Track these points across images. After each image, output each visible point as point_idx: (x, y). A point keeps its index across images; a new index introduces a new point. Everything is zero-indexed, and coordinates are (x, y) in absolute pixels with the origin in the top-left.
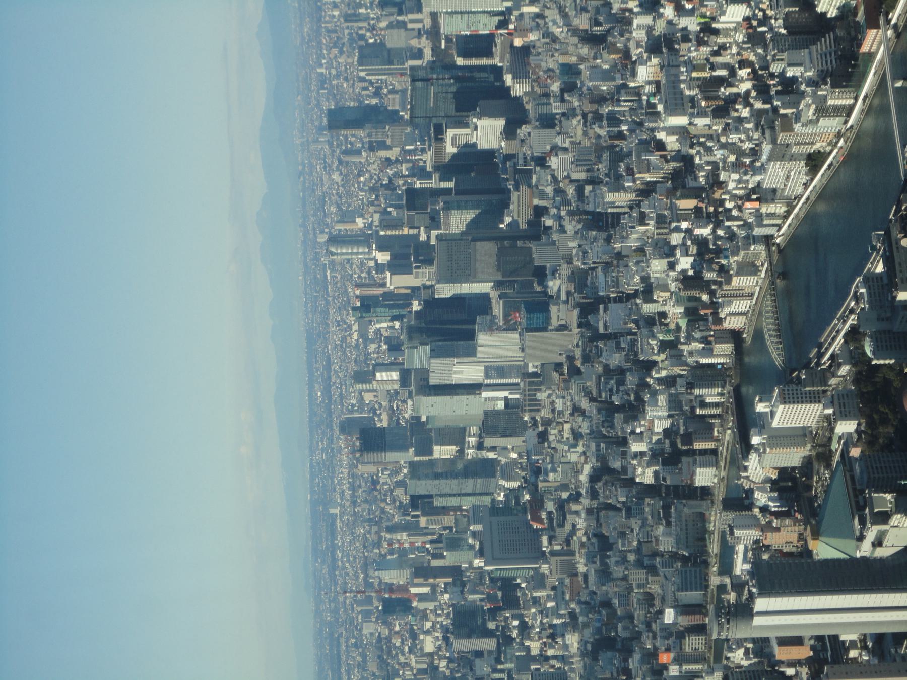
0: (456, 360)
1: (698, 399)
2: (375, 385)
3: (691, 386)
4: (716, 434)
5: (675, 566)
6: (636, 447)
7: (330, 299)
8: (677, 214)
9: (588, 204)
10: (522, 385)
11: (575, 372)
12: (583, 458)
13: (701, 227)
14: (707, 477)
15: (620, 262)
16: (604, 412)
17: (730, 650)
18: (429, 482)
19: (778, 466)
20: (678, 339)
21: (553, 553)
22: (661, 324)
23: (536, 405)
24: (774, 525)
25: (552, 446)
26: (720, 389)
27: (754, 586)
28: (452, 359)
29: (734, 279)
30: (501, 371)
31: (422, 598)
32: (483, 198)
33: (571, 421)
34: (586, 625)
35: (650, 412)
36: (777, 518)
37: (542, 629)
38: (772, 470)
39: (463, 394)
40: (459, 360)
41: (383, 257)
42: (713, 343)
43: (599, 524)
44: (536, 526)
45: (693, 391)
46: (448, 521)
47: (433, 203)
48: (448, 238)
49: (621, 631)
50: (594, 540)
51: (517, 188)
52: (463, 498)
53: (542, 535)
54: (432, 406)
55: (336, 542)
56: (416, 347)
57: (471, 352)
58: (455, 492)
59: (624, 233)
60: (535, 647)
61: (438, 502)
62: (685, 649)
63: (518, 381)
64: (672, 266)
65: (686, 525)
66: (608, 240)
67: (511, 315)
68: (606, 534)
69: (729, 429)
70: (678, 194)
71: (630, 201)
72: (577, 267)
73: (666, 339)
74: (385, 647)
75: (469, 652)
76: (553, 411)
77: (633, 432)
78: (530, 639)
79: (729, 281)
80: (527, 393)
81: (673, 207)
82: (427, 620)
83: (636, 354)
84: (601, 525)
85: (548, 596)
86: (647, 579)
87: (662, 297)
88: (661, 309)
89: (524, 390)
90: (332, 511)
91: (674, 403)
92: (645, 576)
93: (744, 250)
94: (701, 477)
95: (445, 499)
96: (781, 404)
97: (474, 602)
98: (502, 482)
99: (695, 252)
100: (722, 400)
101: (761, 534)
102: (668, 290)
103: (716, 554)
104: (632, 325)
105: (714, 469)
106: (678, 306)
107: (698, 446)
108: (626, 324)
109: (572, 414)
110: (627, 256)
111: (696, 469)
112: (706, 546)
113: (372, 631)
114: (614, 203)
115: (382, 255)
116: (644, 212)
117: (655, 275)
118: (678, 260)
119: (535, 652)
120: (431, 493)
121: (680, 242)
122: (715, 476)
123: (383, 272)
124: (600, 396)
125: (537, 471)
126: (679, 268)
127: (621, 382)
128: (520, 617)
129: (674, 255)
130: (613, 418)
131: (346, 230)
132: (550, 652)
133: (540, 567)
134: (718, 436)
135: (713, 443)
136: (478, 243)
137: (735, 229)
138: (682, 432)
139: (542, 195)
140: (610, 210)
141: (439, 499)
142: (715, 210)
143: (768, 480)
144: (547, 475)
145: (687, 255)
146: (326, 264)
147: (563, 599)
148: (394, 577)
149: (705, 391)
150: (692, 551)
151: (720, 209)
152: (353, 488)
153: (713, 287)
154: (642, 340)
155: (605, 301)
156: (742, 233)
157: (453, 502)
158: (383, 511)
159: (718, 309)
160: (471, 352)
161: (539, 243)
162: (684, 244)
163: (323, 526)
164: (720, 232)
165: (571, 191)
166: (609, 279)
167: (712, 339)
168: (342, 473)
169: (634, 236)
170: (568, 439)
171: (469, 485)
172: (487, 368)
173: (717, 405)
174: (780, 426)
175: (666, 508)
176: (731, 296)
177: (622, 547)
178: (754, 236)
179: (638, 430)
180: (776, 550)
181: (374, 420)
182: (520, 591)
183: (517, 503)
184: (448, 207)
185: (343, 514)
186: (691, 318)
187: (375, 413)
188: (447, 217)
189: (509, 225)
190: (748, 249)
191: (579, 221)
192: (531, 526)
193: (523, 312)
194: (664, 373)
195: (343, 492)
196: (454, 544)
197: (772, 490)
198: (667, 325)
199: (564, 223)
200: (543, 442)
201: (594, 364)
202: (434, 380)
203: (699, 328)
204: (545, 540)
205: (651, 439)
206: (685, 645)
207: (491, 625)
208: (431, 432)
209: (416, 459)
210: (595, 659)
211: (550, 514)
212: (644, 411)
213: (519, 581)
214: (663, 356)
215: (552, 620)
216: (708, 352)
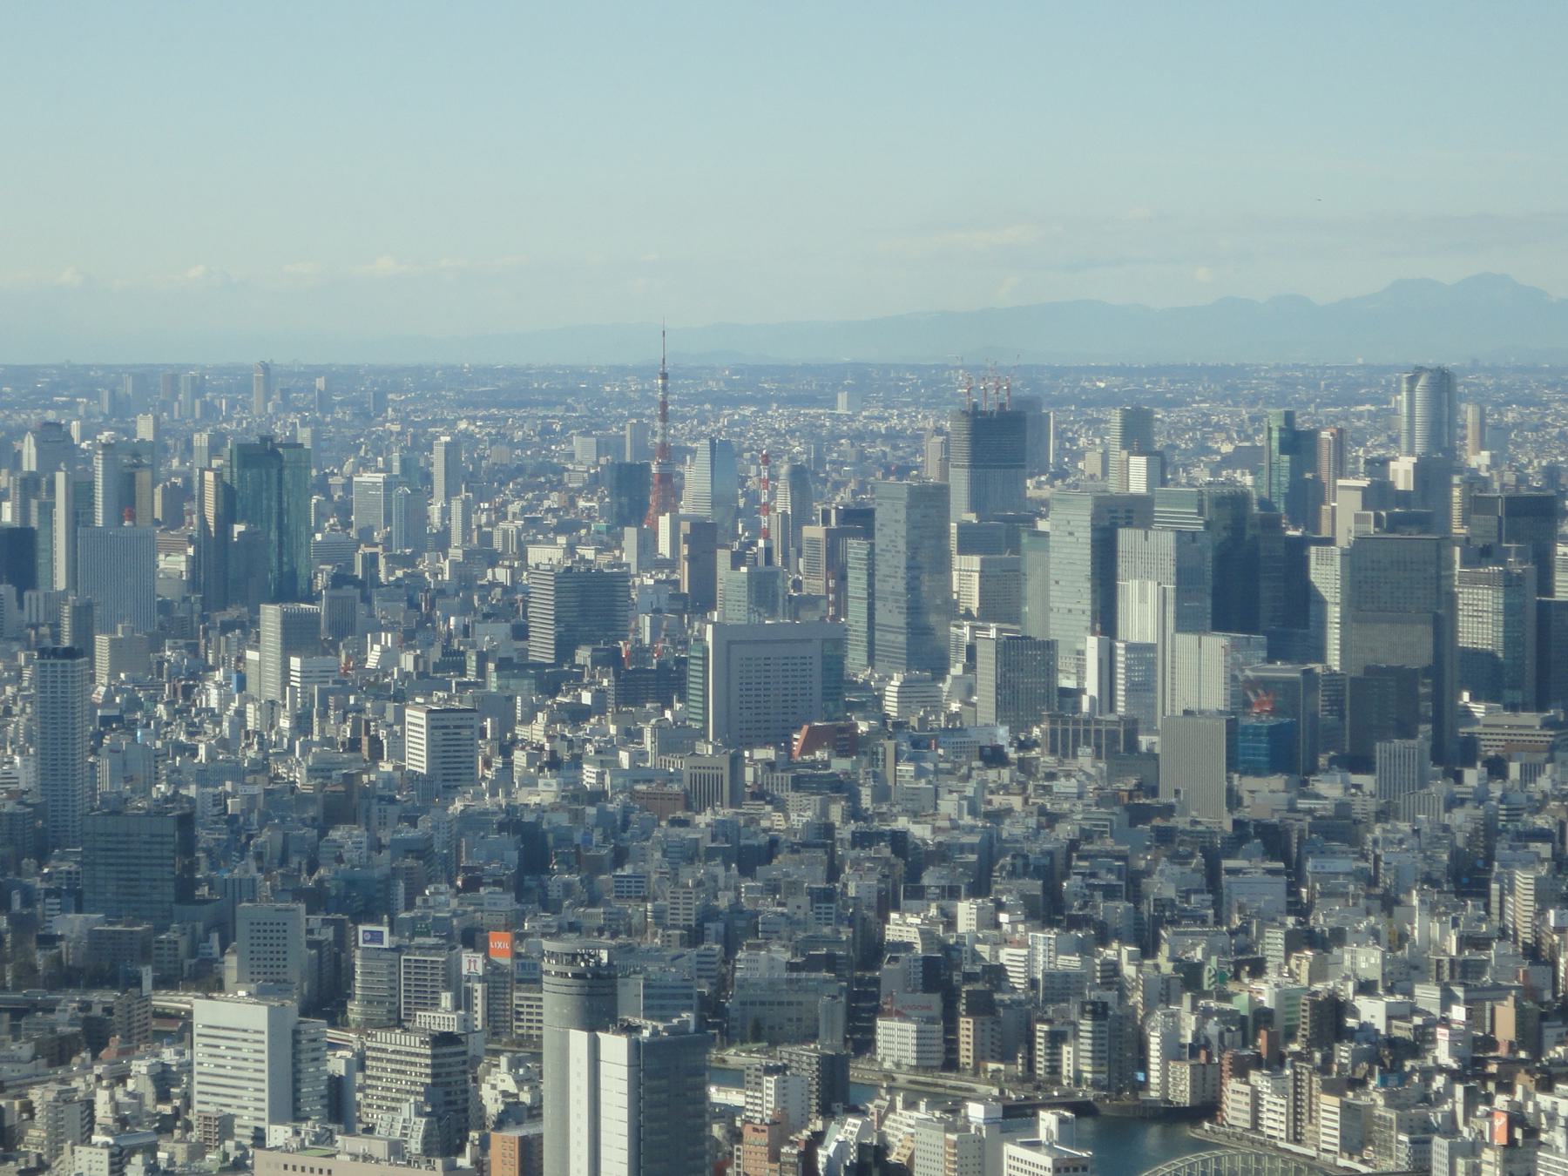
0: (1171, 587)
1: (1069, 1029)
2: (1118, 454)
3: (1099, 1012)
4: (992, 1066)
5: (703, 981)
6: (966, 913)
7: (1311, 409)
8: (1482, 1000)
9: (1511, 847)
10: (1112, 717)
11: (1138, 814)
12: (946, 824)
13: (1452, 1043)
14: (896, 1046)
15: (1378, 902)
16: (1046, 861)
17: (514, 1065)
18: (902, 529)
19: (917, 1161)
20: (1207, 995)
21: (736, 763)
22: (1239, 965)
23: (1065, 746)
24: (785, 1149)
25: (974, 773)
26: (1089, 1076)
27: (655, 1032)
28: (1174, 579)
29: (1335, 1101)
30: (1142, 689)
31: (647, 542)
32: (1530, 662)
33: (1029, 809)
34: (577, 816)
35: (1043, 939)
36: (800, 1154)
37: (571, 741)
38: (908, 1153)
39: (1094, 602)
40: (1171, 595)
41: (1402, 472)
42: (1193, 1062)
43: (794, 849)
44: (799, 737)
45: (1088, 1016)
46: (816, 585)
47: (1519, 553)
48: (1443, 582)
49: (561, 877)
50: (763, 839)
51: (1547, 724)
52: (865, 605)
53: (778, 748)
54: (1071, 534)
55: (775, 406)
56: (1200, 513)
57: (1186, 622)
58: (878, 586)
59: (1442, 909)
60: (536, 731)
61: (855, 549)
62: (519, 989)
63: (1121, 708)
64: (1366, 988)
65: (790, 1004)
66: (1429, 880)
67: (1267, 694)
68: (775, 862)
69: (1002, 1092)
70: (1528, 1004)
71: (1515, 930)
72: (1370, 831)
73: (1206, 975)
74: (543, 479)
75: (525, 616)
76: (1051, 776)
77: (1000, 907)
78: (551, 721)
79: (1329, 1088)
80: (1093, 728)
81: (1498, 992)
82: (598, 551)
83: (1173, 922)
84: (797, 852)
85: (643, 755)
86: (675, 927)
87: (1298, 966)
88: (1270, 966)
89: (1098, 722)
90: (842, 398)
91: (1059, 987)
92: (681, 923)
93: (1399, 1119)
94: (896, 1033)
95: (863, 565)
96: (1055, 1161)
97: (637, 630)
98: (896, 681)
99: (1397, 1033)
100: (1065, 1082)
101: (767, 1120)
102: (1311, 980)
103: (724, 1061)
104: (1237, 921)
105: (914, 1062)
106: (1277, 995)
107: (966, 1026)
108: (1241, 909)
109: (1042, 811)
110: (1390, 915)
111: (916, 1022)
112: (743, 1041)
113: (578, 456)
114: (1512, 891)
115: (1407, 472)
116: (1488, 946)
117: (1347, 957)
118: (1380, 998)
119: (521, 732)
120: (877, 535)
121: (1420, 1006)
122: (898, 1065)
123: (1368, 474)
124: (1080, 858)
125: (919, 745)
126: (1362, 1003)
127: (1110, 892)
128: (599, 707)
129: (1390, 991)
130: (1032, 877)
131: (1464, 438)
132: (519, 757)
133: (707, 742)
134: (985, 1071)
135: (971, 1061)
136: (1430, 629)
137: (1446, 1108)
138: (997, 996)
139: (1530, 773)
140: (1495, 887)
141: (863, 553)
142: (1491, 1076)
143: (882, 1149)
144: (910, 759)
145: (1389, 1018)
146: (1389, 403)
147: (637, 782)
148: (696, 478)
149: (1086, 1044)
150: (733, 1014)
151: (1491, 1086)
152: (892, 436)
153: (1318, 1055)
154: (1205, 934)
155: (1295, 876)
156: (1436, 1117)
157: (857, 584)
158: (837, 486)
159: (1268, 1068)
160: (1186, 622)
161: (1427, 754)
162: (1415, 1011)
163: (809, 383)
164: (1439, 1082)
165: (1541, 822)
166: (1341, 880)
167: (1203, 1058)
168: (925, 417)
169: (1435, 930)
170: (990, 802)
171: (892, 616)
172: (1151, 648)
173: (1054, 1069)
174: (1006, 1160)
175: (830, 962)
176: (1296, 1093)
177: (747, 887)
178: (1428, 1142)
179: (1004, 918)
180: (731, 1154)
181: (1040, 474)
182: (656, 709)
183: (851, 707)
184: (1511, 583)
185: (837, 418)
186: (1250, 1022)
187: (1055, 476)
188: (1489, 581)
189: (1467, 713)
190: (1401, 1129)
191: (1470, 841)
192: (798, 728)
193: (1273, 721)
194: (1129, 970)
195: (881, 419)
196: (763, 589)
197: (862, 1148)
198: (1236, 977)
199: (1469, 805)
200: (982, 757)
201: (1153, 852)
202: (1127, 538)
203: (1229, 1030)
204: (768, 753)
205: (983, 941)
206: (529, 991)
207: (583, 655)
208: (1011, 553)
209: (953, 525)
210: (502, 827)
211: (827, 765)
212: (1042, 928)
213: (678, 706)
214: (1167, 967)
215: (591, 762)
216: (1173, 1051)
